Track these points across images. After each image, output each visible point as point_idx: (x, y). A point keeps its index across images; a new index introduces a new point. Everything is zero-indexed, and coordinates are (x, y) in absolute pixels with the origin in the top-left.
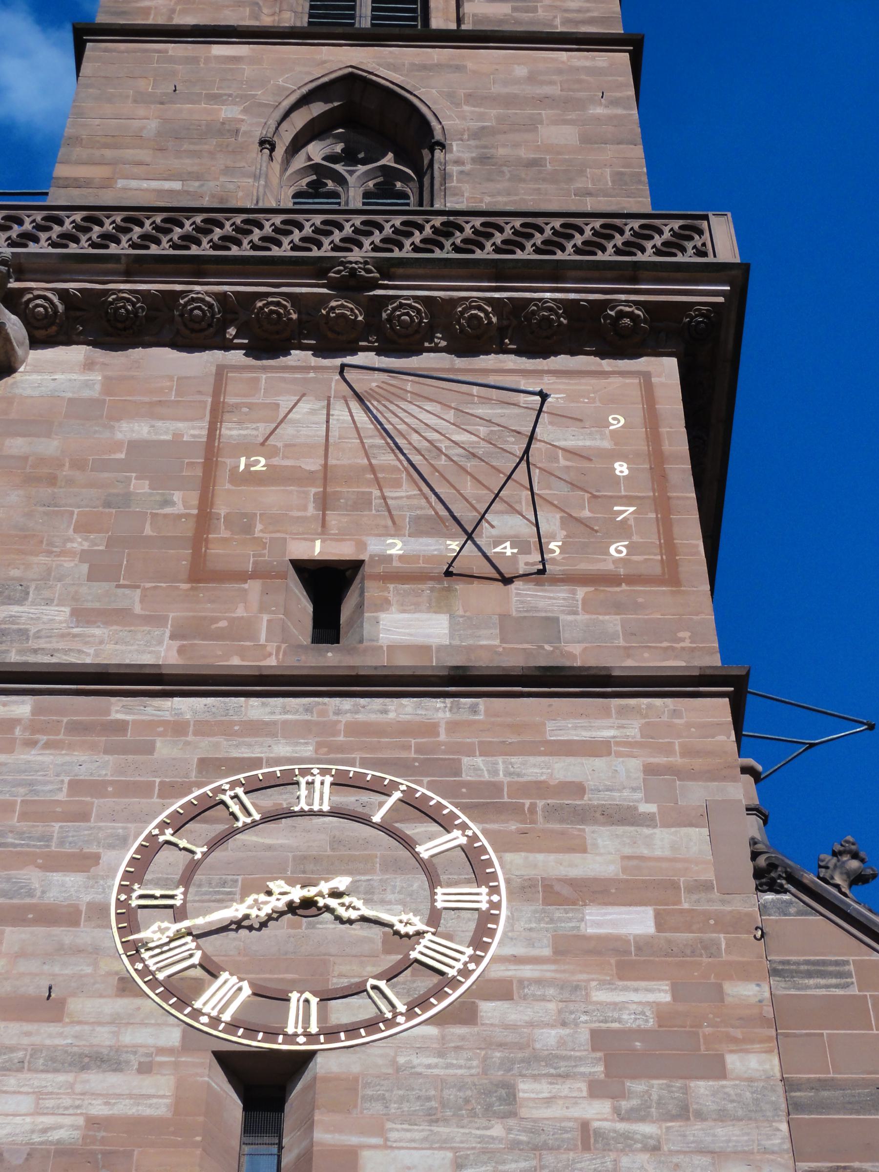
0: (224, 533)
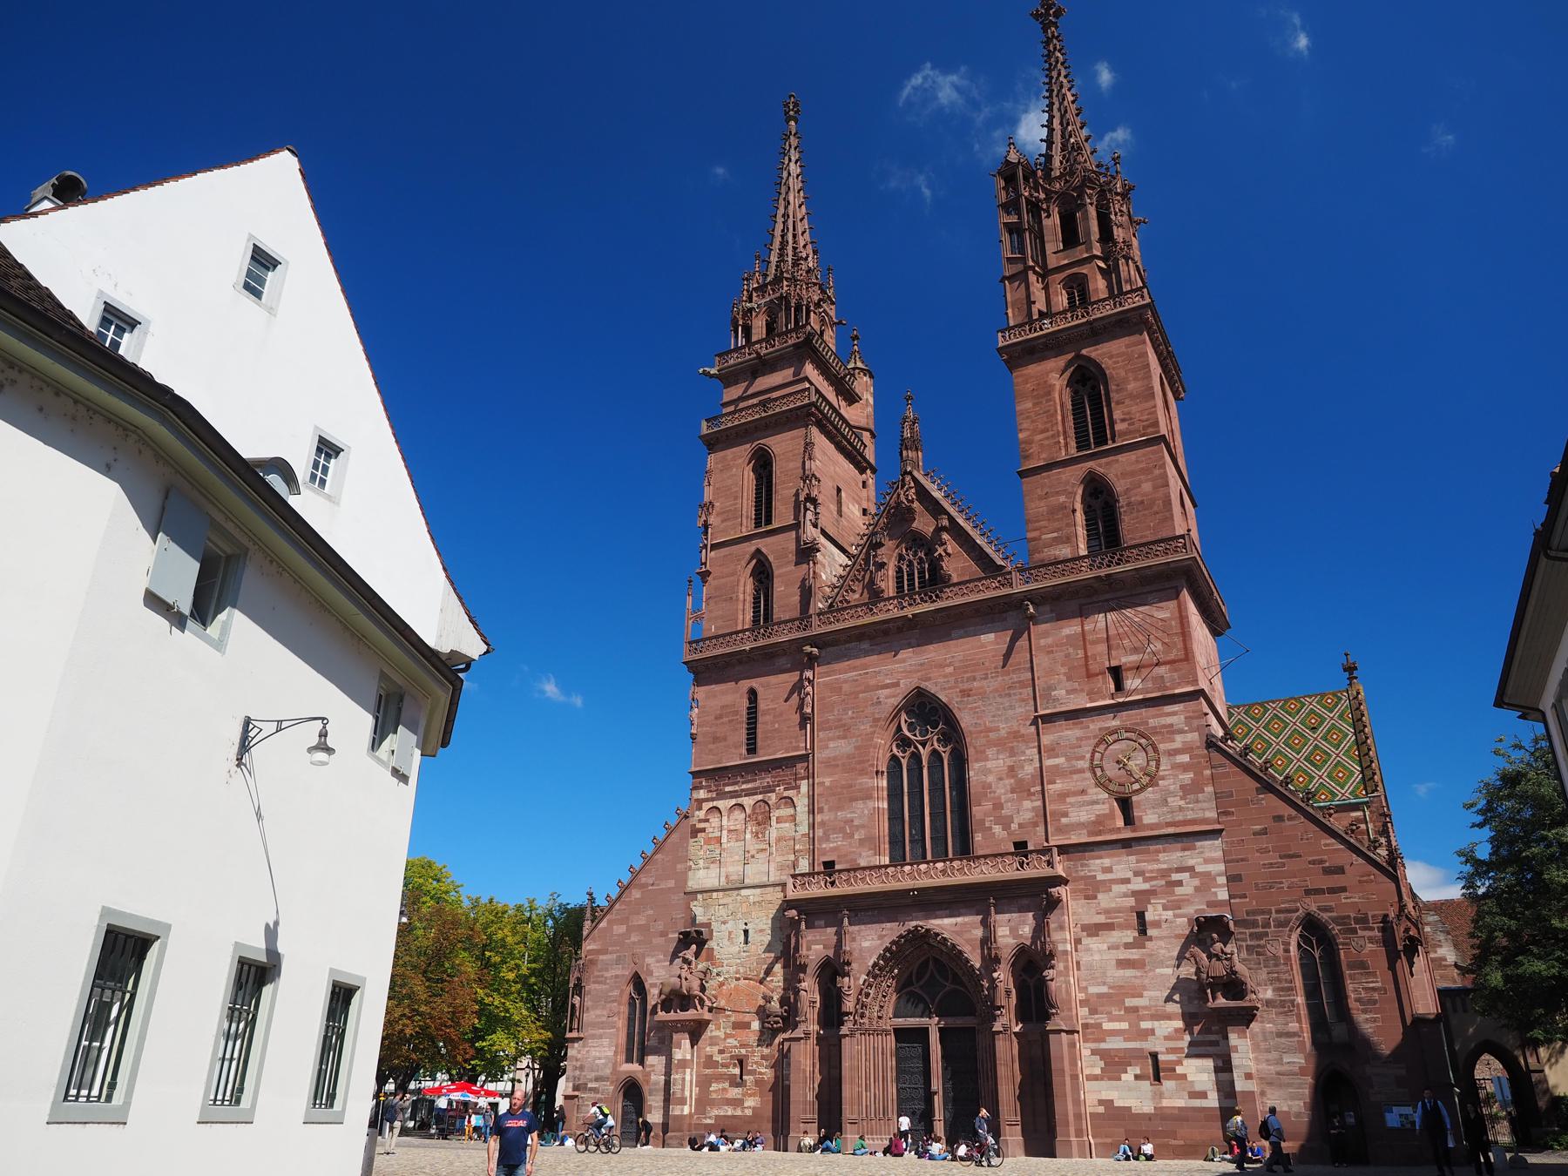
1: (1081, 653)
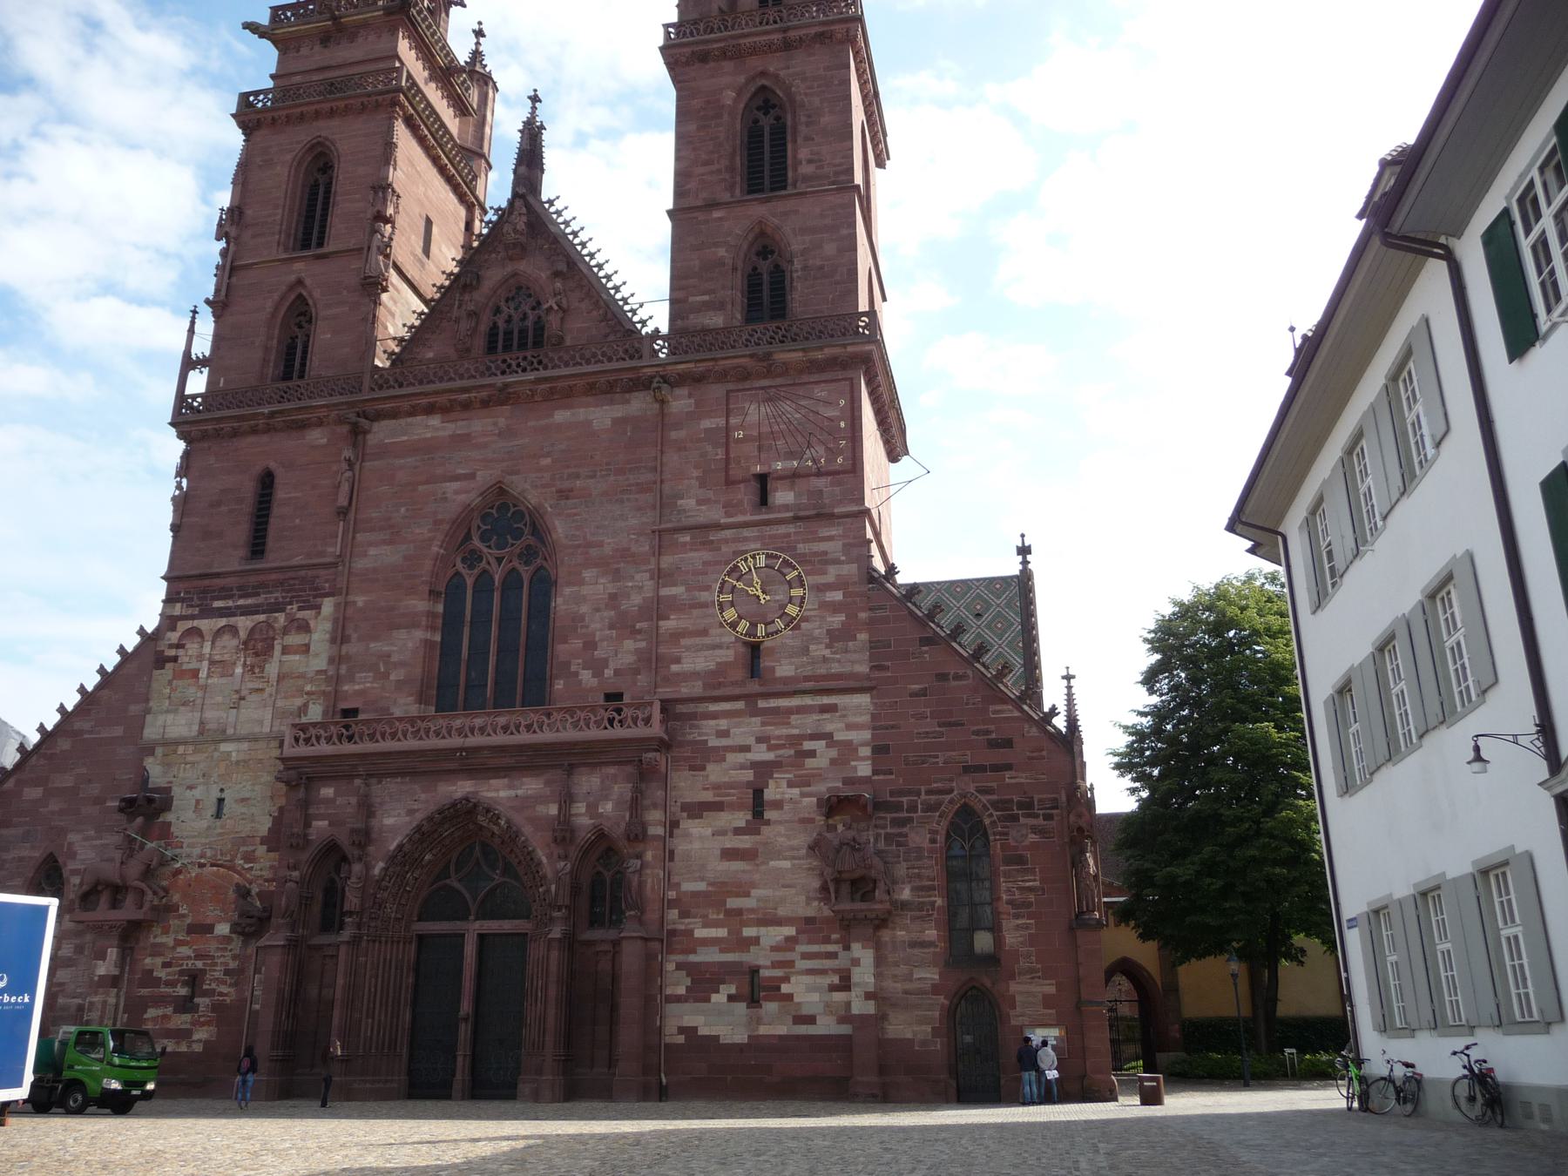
0: (734, 466)
1: (721, 454)
